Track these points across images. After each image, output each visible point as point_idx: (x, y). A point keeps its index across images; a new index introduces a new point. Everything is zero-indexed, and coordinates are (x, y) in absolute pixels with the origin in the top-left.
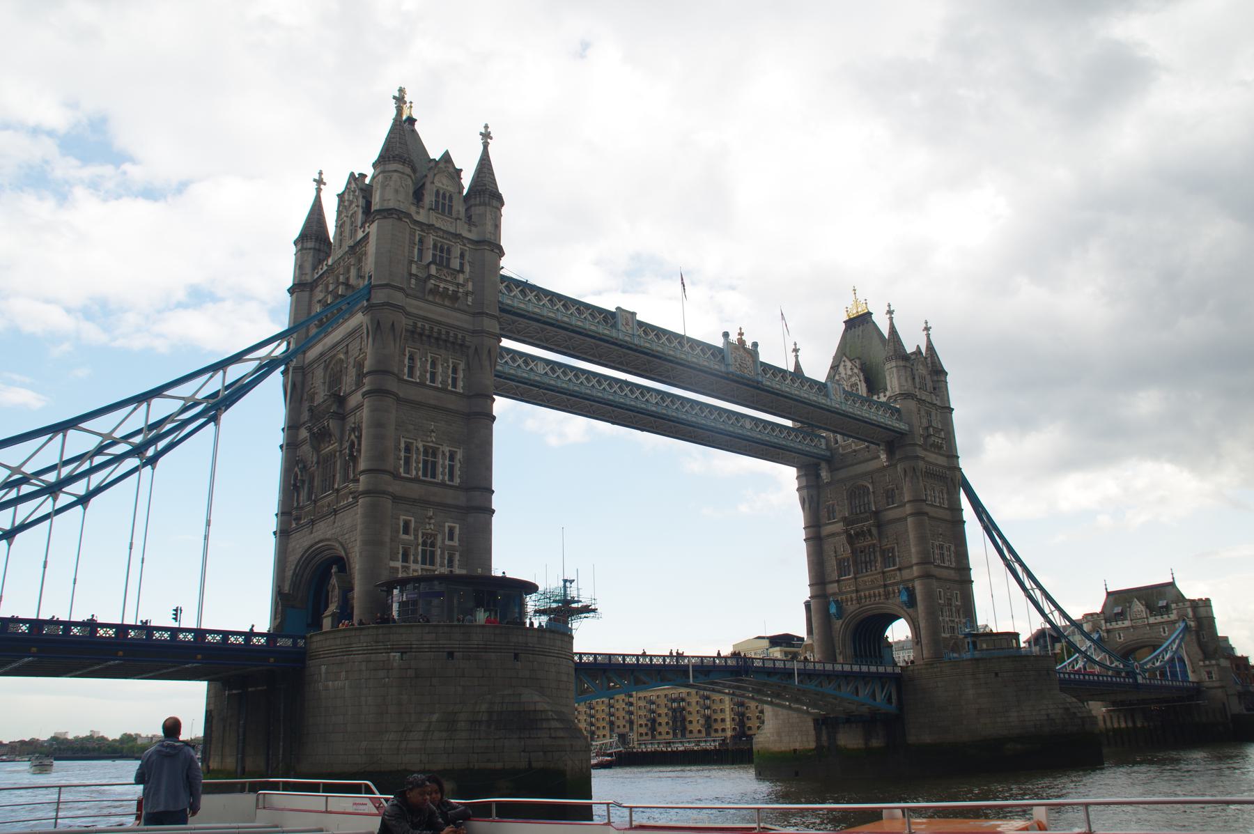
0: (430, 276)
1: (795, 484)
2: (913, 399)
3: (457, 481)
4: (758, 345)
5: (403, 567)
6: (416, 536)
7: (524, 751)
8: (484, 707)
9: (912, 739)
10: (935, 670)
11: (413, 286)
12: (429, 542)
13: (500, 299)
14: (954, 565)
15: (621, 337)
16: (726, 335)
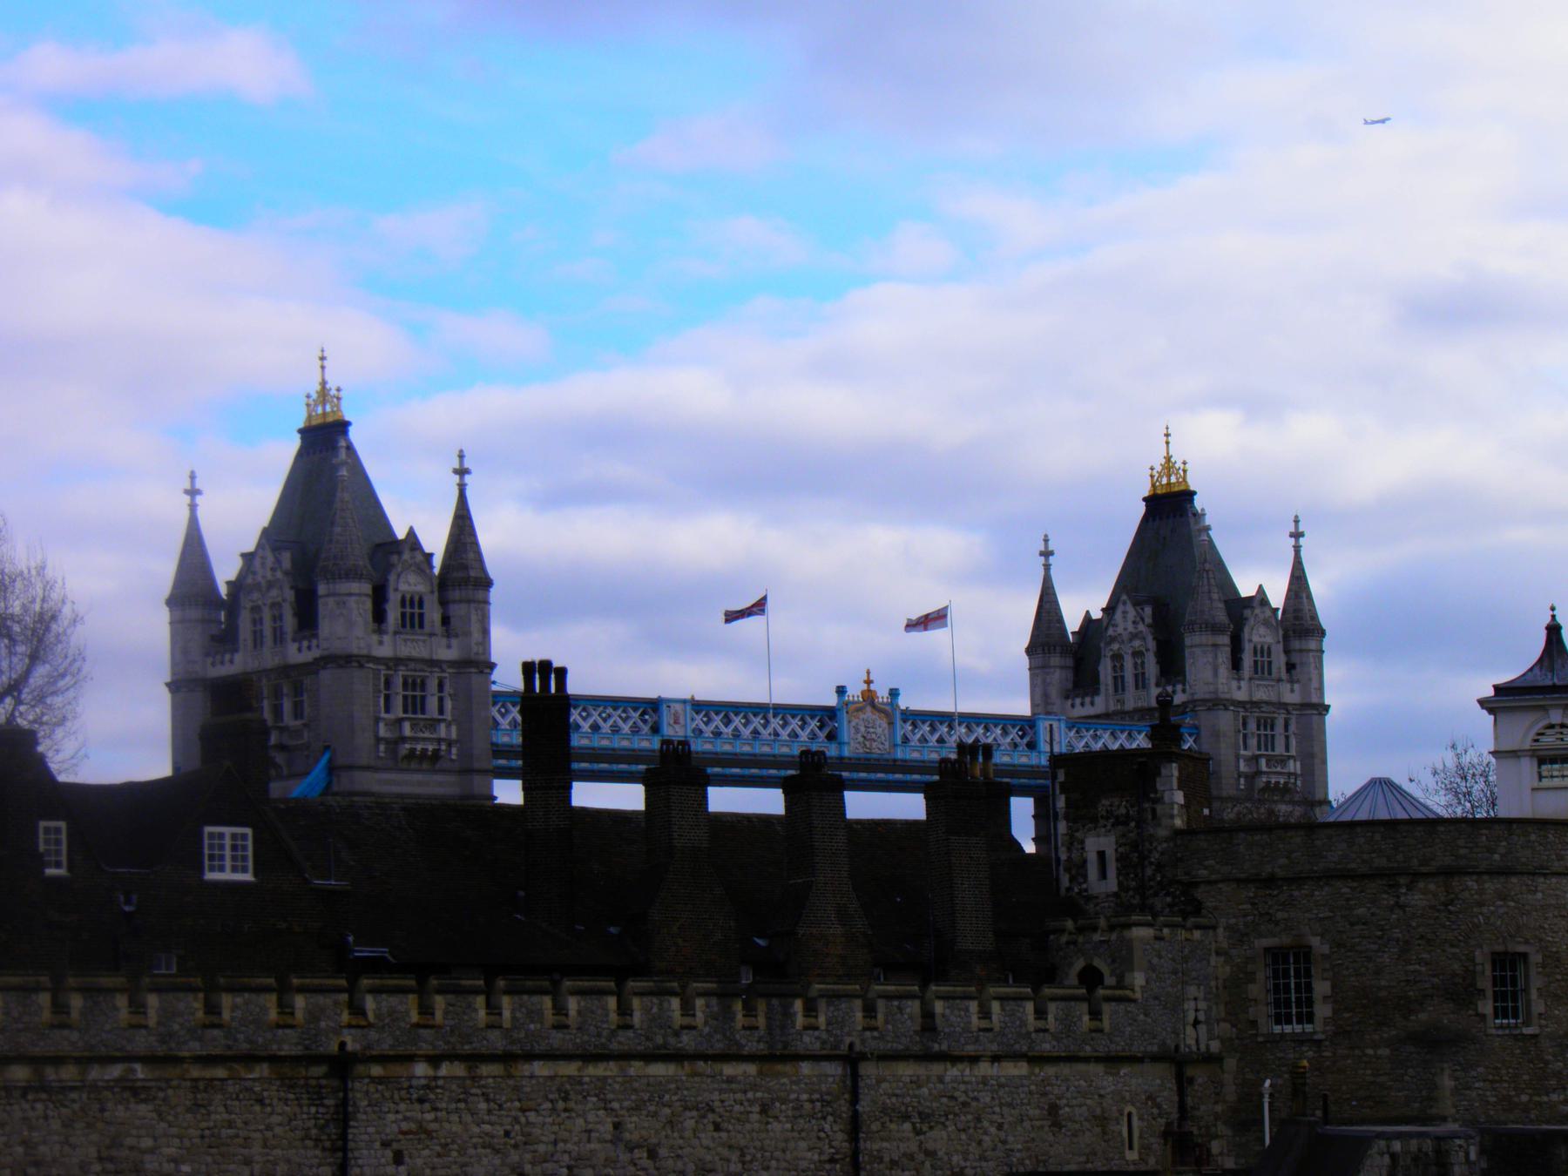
0: (404, 739)
2: (1226, 709)
4: (898, 695)
11: (382, 755)
13: (494, 740)
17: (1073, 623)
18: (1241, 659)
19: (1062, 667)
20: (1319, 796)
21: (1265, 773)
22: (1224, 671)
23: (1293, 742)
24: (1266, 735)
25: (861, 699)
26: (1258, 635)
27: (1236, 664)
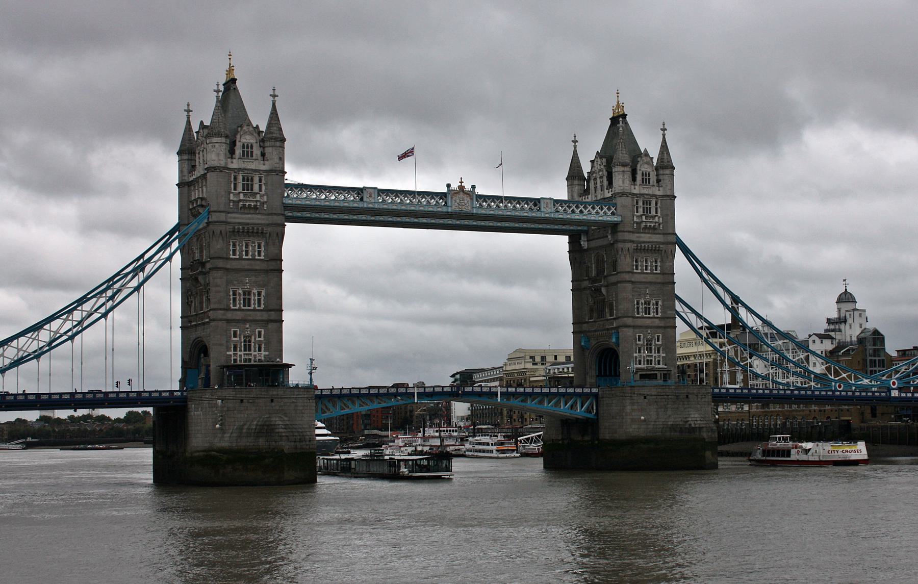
0: (240, 201)
1: (566, 247)
2: (627, 196)
3: (262, 307)
4: (475, 188)
5: (234, 354)
6: (240, 338)
7: (267, 441)
8: (255, 423)
9: (601, 437)
10: (613, 392)
11: (232, 207)
12: (248, 339)
13: (284, 201)
14: (660, 314)
15: (365, 206)
16: (448, 186)
17: (586, 168)
18: (636, 177)
19: (578, 185)
20: (671, 231)
21: (644, 221)
22: (628, 182)
23: (659, 210)
24: (647, 207)
25: (458, 189)
26: (642, 168)
27: (634, 179)
